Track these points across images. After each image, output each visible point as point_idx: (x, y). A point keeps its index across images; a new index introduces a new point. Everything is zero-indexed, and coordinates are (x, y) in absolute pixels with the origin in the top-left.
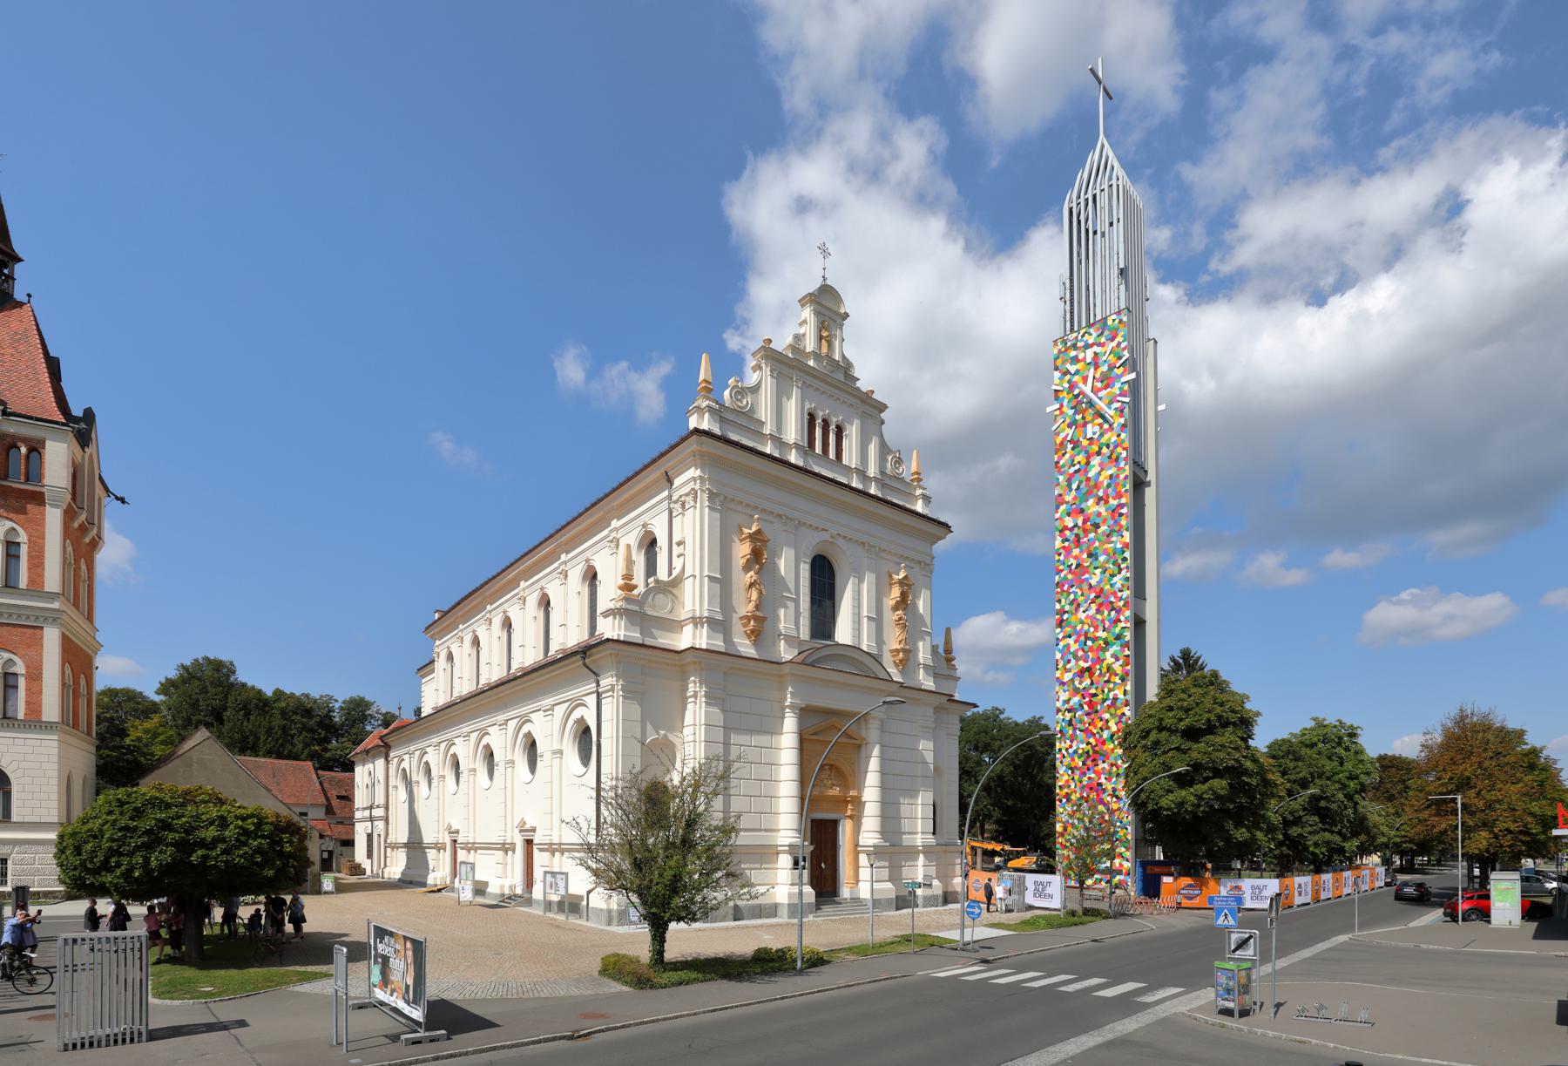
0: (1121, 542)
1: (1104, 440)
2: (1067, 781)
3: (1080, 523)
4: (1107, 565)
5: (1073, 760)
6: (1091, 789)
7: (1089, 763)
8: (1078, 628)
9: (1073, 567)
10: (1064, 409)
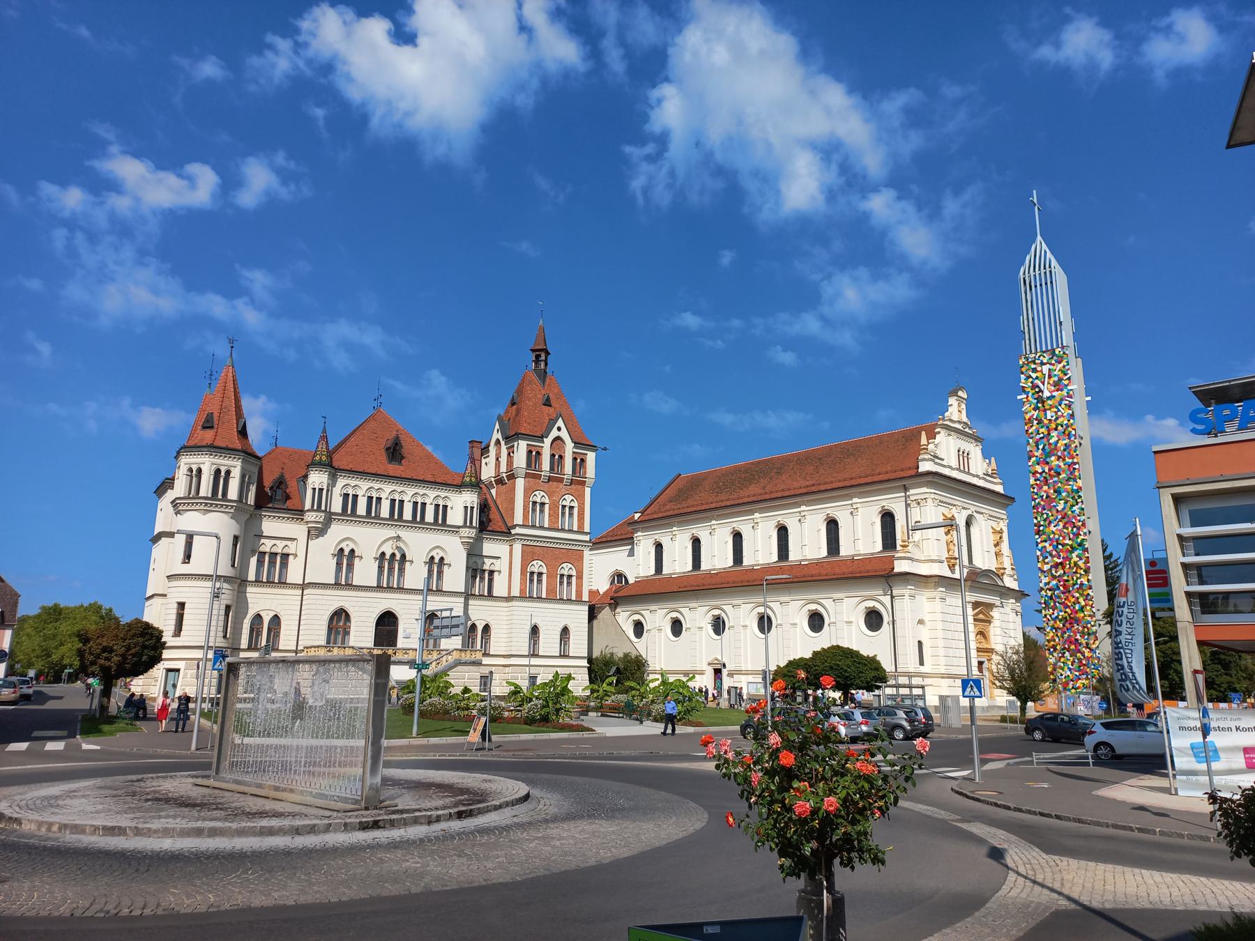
1: (1059, 421)
2: (1053, 637)
3: (1047, 471)
5: (1055, 622)
6: (1071, 642)
7: (1068, 625)
9: (1044, 497)
10: (1030, 398)
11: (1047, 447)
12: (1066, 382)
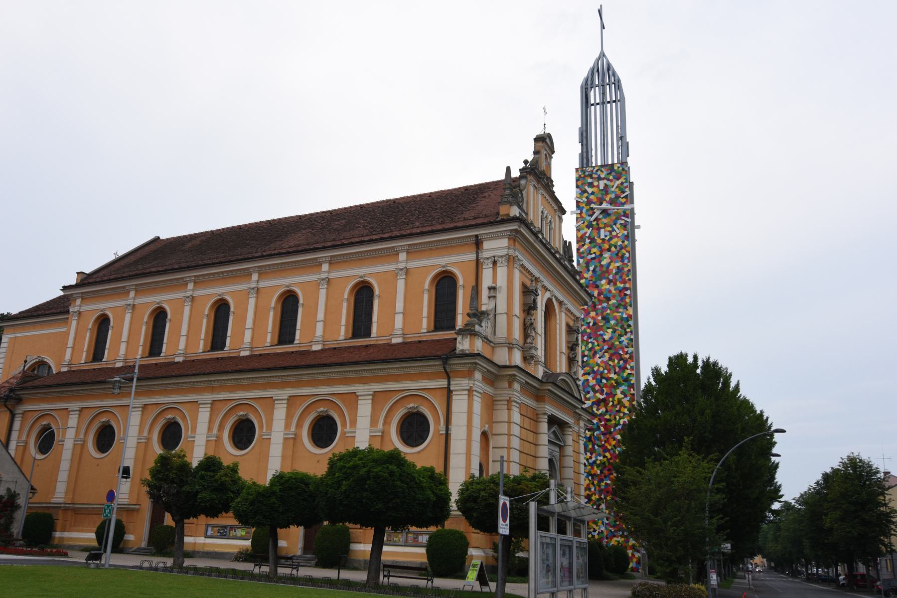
0: (626, 314)
1: (613, 242)
4: (616, 328)
5: (593, 468)
6: (608, 492)
7: (606, 472)
9: (591, 324)
10: (584, 215)
11: (598, 269)
12: (623, 200)
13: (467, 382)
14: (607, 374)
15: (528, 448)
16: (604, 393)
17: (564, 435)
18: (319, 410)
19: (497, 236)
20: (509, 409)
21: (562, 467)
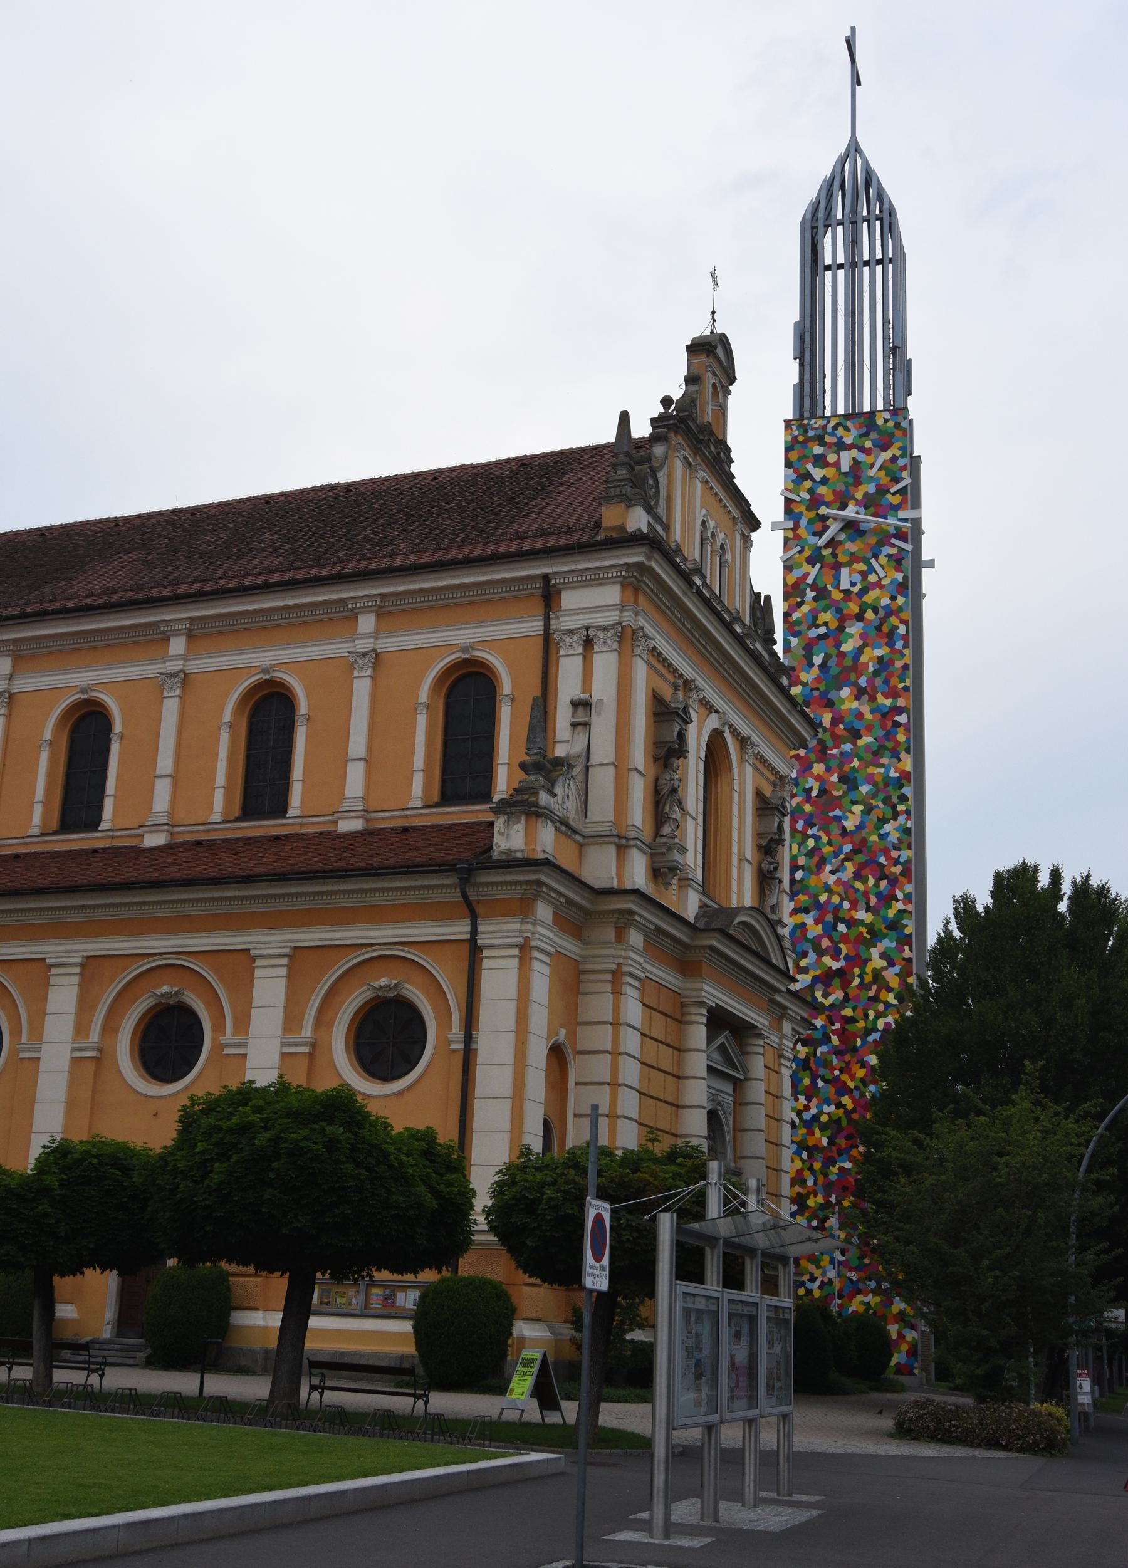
0: (896, 768)
4: (874, 802)
5: (811, 1133)
6: (845, 1189)
7: (842, 1142)
8: (823, 898)
9: (814, 793)
10: (802, 532)
11: (832, 663)
13: (517, 926)
14: (849, 910)
15: (659, 1085)
16: (842, 956)
17: (745, 1054)
18: (158, 992)
19: (596, 579)
20: (617, 992)
21: (738, 1130)
